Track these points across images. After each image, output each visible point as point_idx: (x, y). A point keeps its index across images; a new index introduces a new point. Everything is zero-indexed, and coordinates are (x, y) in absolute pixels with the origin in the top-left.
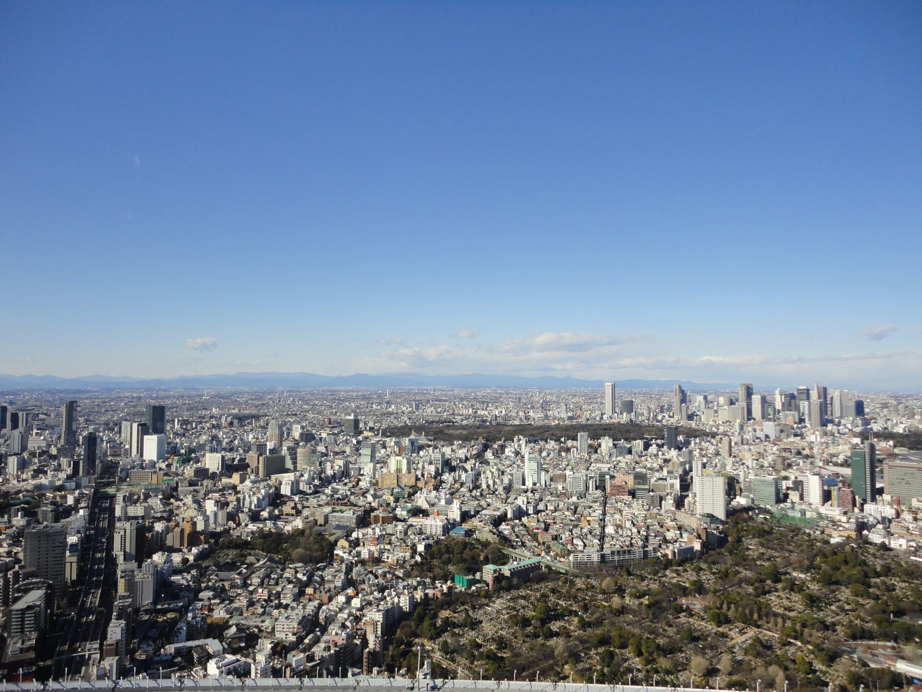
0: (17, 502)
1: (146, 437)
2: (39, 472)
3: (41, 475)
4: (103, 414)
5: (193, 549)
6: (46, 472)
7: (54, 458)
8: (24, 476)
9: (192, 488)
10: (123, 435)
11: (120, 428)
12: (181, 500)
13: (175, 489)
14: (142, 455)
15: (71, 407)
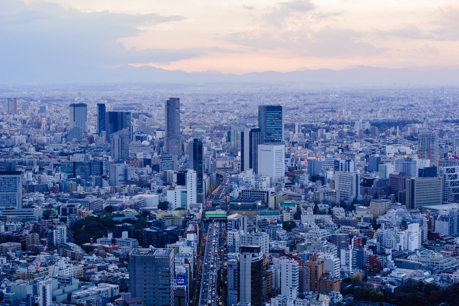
0: (120, 219)
1: (260, 147)
2: (143, 185)
3: (143, 189)
4: (210, 115)
5: (321, 296)
6: (149, 186)
7: (156, 168)
8: (126, 190)
9: (318, 217)
10: (233, 143)
11: (229, 133)
12: (306, 231)
13: (298, 215)
14: (256, 171)
15: (172, 105)
